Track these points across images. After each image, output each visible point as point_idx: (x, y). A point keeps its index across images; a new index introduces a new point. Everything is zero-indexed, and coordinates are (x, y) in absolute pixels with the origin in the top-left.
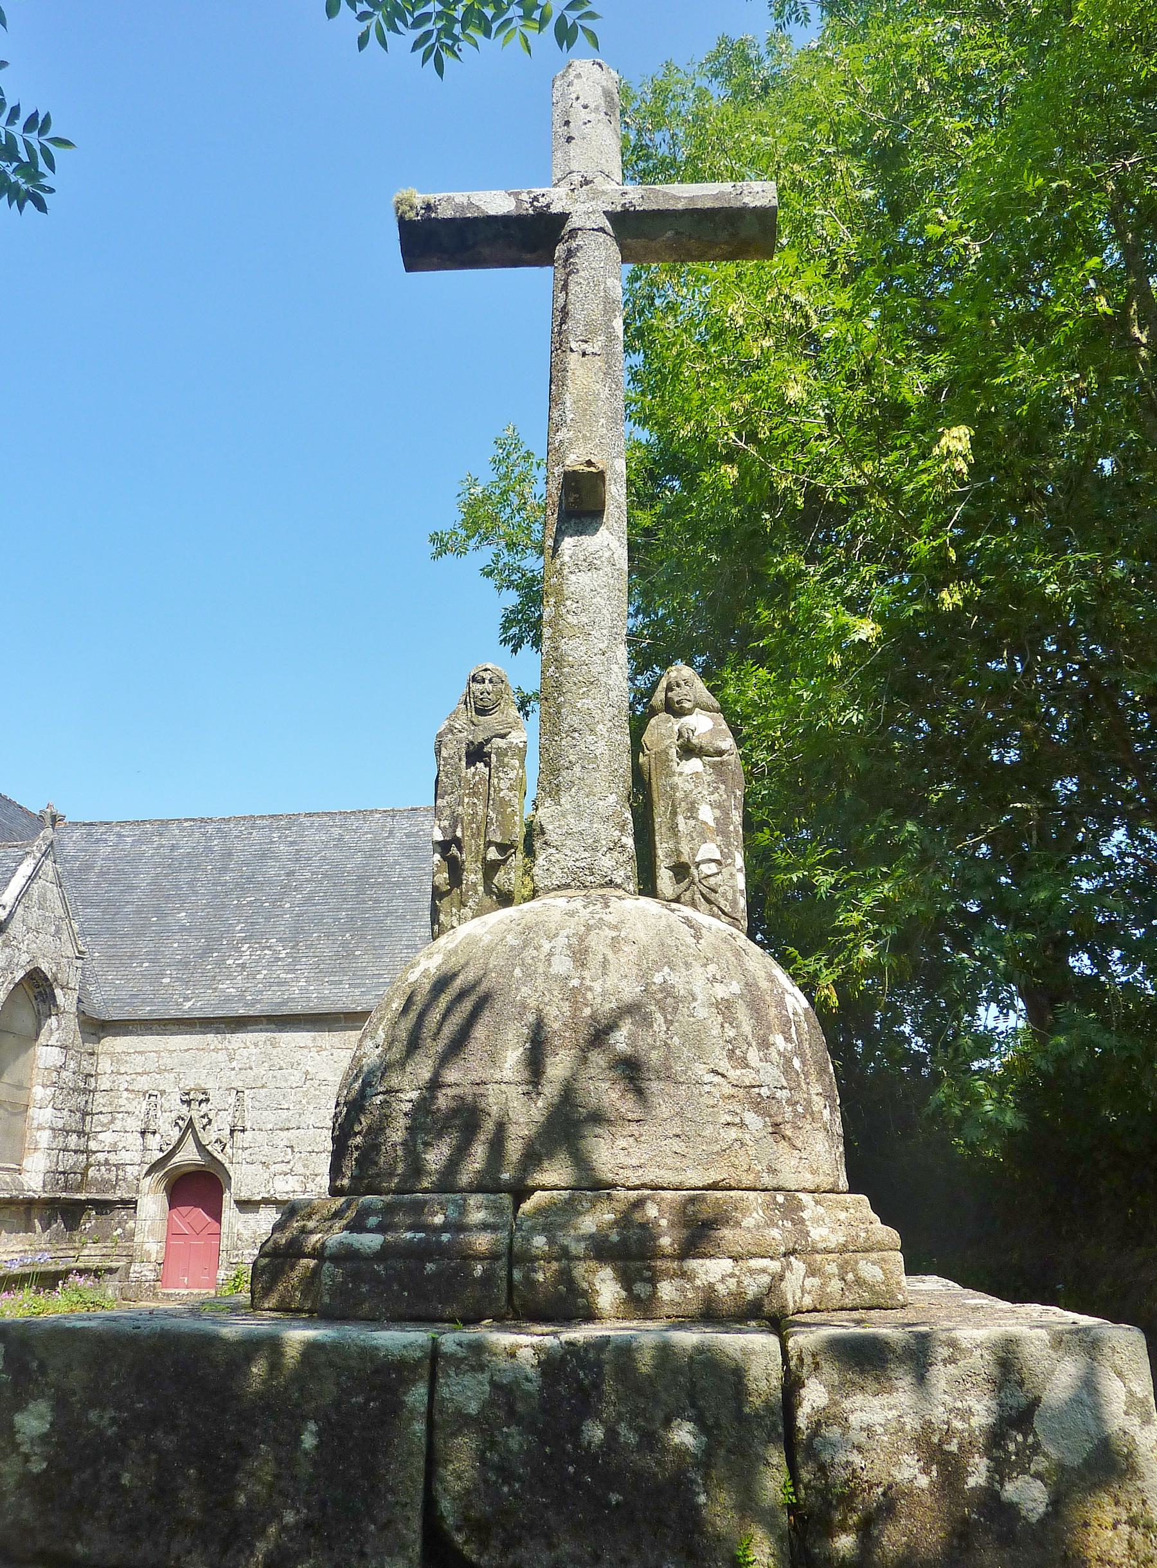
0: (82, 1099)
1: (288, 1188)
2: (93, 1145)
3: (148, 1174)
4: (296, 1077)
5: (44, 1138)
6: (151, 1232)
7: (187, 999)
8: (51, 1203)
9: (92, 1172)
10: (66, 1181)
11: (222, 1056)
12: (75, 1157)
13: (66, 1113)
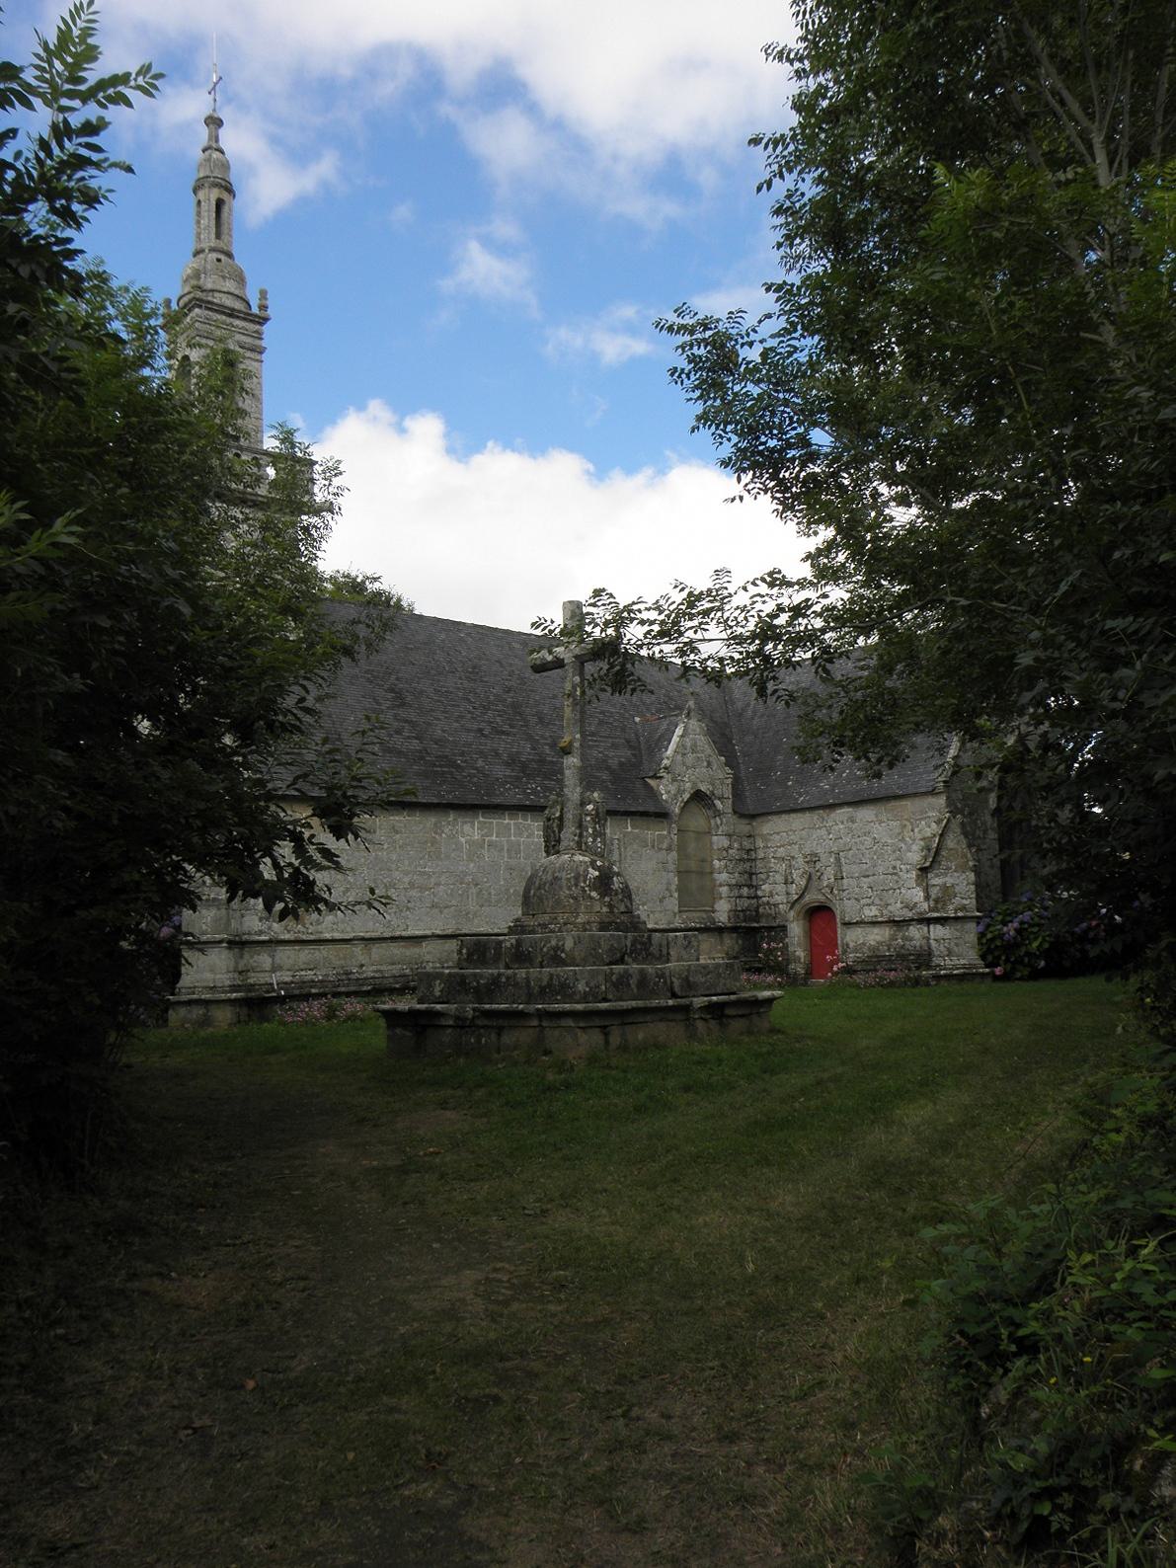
1: (872, 914)
2: (759, 893)
3: (791, 908)
4: (868, 841)
5: (724, 890)
6: (799, 945)
8: (734, 929)
9: (761, 910)
10: (745, 916)
11: (823, 832)
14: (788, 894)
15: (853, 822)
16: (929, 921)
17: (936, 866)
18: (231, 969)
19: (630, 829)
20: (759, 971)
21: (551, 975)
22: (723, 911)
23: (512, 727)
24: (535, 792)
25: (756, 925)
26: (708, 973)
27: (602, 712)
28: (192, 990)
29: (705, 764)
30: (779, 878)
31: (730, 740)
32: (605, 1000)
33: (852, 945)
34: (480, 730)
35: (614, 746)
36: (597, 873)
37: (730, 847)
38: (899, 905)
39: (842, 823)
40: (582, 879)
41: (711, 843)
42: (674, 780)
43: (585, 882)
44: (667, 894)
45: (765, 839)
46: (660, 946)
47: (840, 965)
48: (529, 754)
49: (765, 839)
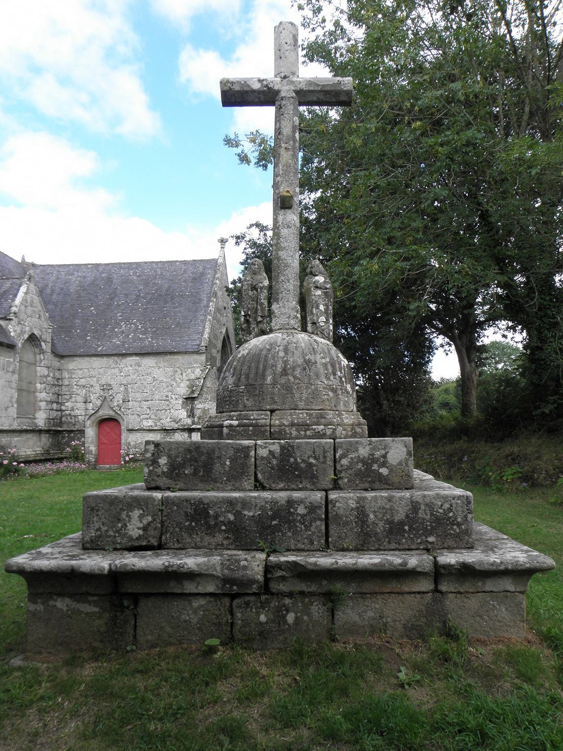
1: (149, 425)
2: (63, 408)
3: (89, 419)
5: (43, 405)
6: (92, 443)
8: (48, 431)
9: (63, 419)
11: (116, 371)
12: (56, 413)
13: (51, 394)
17: (200, 397)
22: (41, 419)
25: (59, 429)
29: (38, 316)
33: (132, 444)
37: (48, 376)
38: (168, 420)
39: (131, 366)
41: (36, 372)
42: (19, 323)
44: (10, 404)
45: (70, 372)
49: (70, 372)
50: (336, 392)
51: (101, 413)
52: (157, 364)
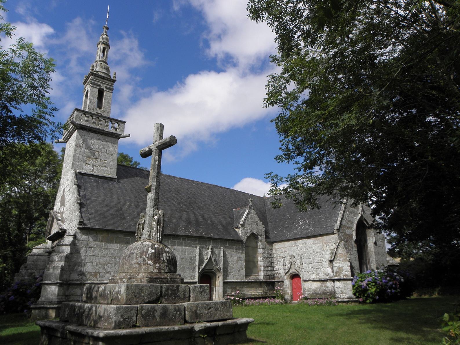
0: (270, 259)
1: (313, 277)
2: (275, 269)
3: (285, 275)
4: (311, 251)
5: (262, 268)
6: (288, 288)
7: (288, 235)
8: (266, 282)
9: (275, 275)
10: (270, 277)
11: (296, 248)
12: (271, 272)
13: (266, 262)
14: (284, 269)
15: (306, 244)
16: (333, 280)
17: (335, 259)
18: (61, 294)
19: (227, 245)
20: (274, 298)
21: (105, 309)
22: (261, 276)
23: (188, 209)
24: (193, 231)
25: (273, 280)
26: (210, 308)
27: (222, 207)
28: (43, 303)
29: (255, 224)
30: (281, 264)
31: (265, 217)
32: (134, 326)
33: (307, 289)
34: (176, 210)
35: (224, 217)
36: (153, 251)
38: (323, 274)
40: (144, 253)
42: (244, 229)
43: (146, 256)
44: (241, 269)
45: (276, 250)
46: (185, 291)
47: (303, 296)
48: (193, 218)
49: (276, 250)
50: (140, 264)
51: (291, 271)
52: (314, 242)
